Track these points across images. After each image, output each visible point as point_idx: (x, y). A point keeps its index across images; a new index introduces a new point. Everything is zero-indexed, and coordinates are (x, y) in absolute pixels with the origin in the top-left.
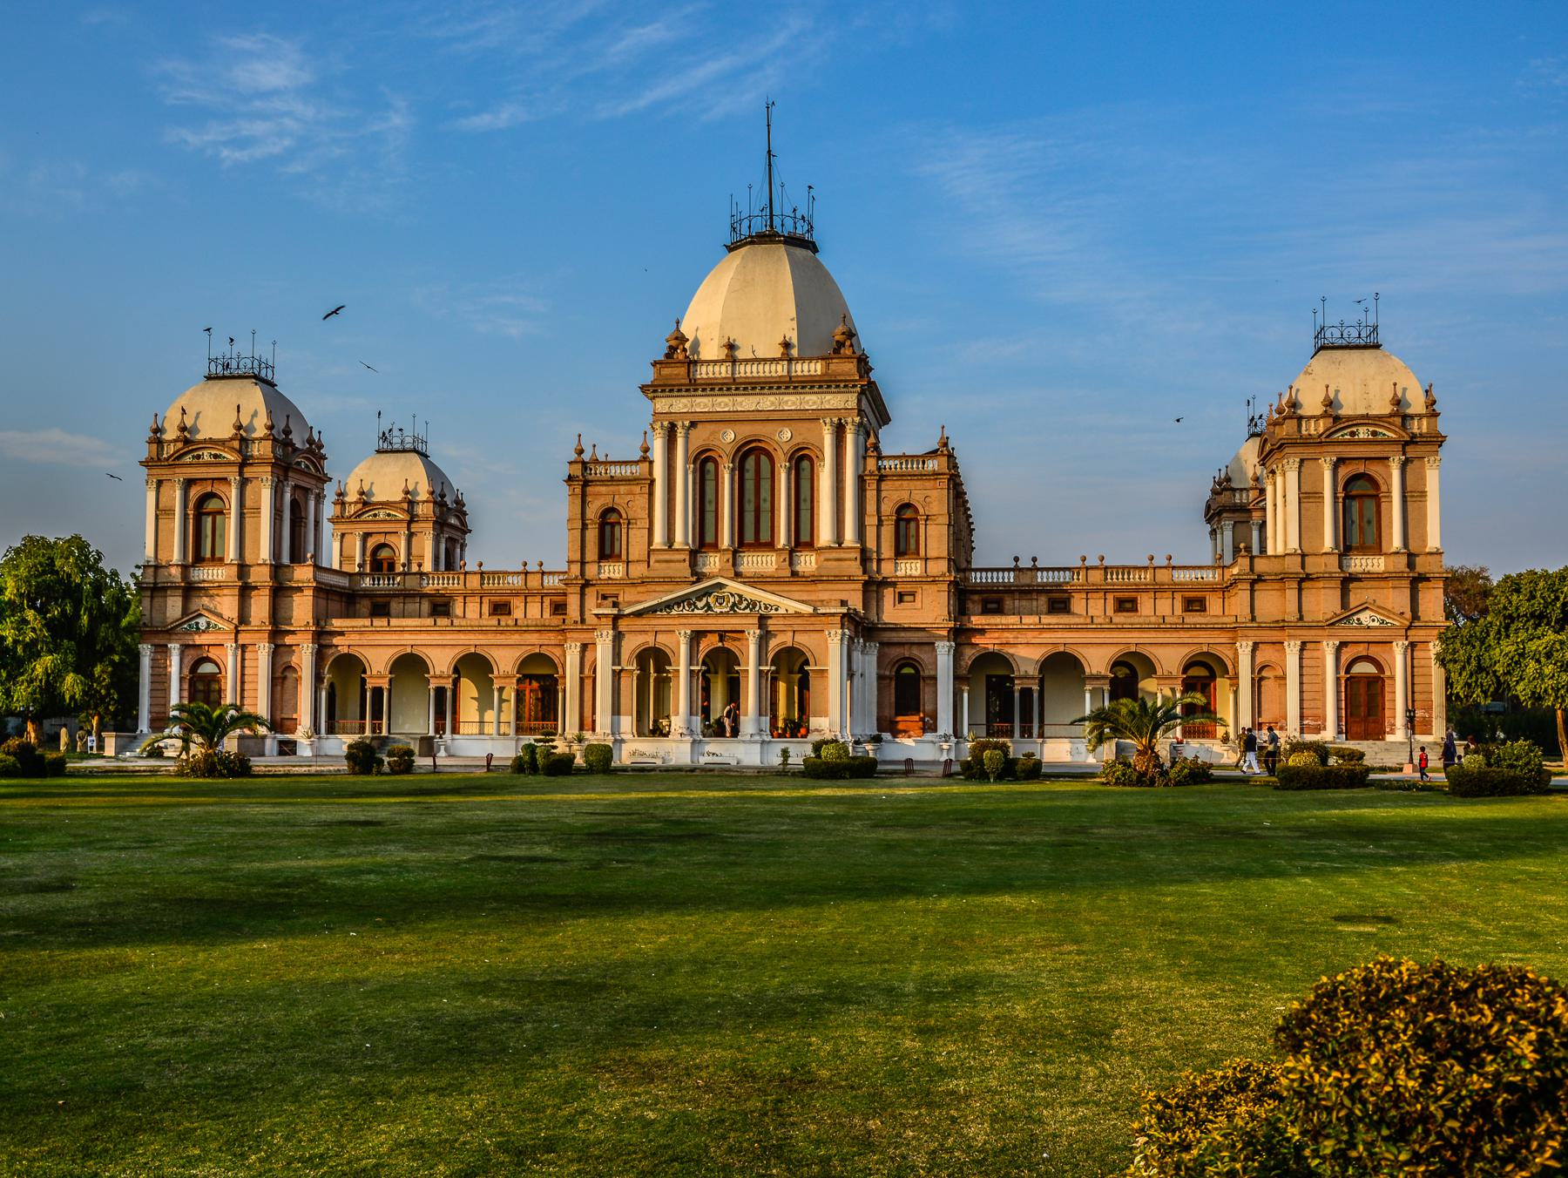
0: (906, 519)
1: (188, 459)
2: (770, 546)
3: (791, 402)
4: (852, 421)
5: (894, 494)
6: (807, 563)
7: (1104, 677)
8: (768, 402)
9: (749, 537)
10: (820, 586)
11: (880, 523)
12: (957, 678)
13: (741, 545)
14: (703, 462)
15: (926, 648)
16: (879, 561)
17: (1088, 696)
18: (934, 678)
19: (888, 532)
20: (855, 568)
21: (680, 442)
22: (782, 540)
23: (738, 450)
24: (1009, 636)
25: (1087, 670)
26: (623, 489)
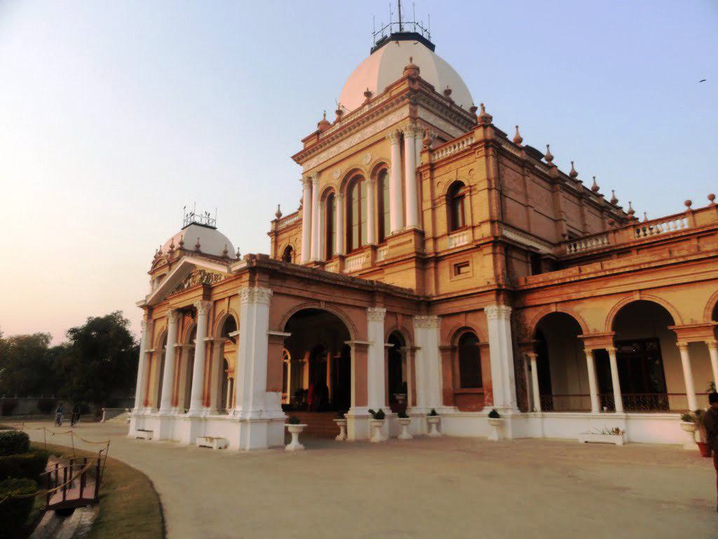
0: (455, 194)
1: (158, 266)
2: (361, 249)
3: (369, 131)
4: (406, 126)
5: (445, 178)
6: (383, 254)
7: (706, 327)
8: (355, 139)
9: (355, 245)
10: (387, 271)
11: (433, 209)
12: (518, 344)
13: (350, 250)
14: (328, 198)
15: (479, 314)
16: (435, 239)
17: (684, 355)
18: (487, 346)
19: (442, 211)
20: (410, 248)
21: (314, 186)
22: (369, 237)
23: (344, 181)
24: (572, 293)
25: (678, 322)
26: (294, 232)
